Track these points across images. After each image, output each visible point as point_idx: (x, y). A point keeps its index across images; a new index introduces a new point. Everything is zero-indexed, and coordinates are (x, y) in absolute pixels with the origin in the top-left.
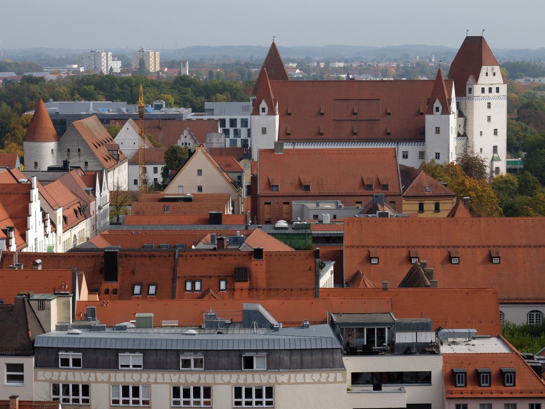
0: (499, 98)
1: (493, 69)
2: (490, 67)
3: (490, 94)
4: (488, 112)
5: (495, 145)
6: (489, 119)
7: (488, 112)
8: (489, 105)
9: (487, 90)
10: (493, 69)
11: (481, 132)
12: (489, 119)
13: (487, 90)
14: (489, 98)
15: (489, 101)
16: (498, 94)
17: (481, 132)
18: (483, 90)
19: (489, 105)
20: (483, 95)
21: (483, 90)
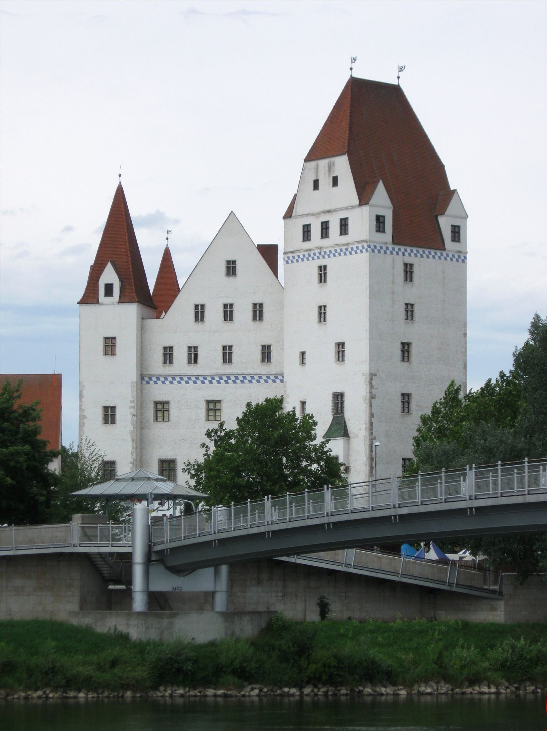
0: (347, 250)
1: (330, 167)
2: (323, 163)
3: (325, 242)
4: (319, 295)
5: (339, 390)
6: (322, 313)
7: (319, 295)
8: (322, 274)
9: (316, 231)
10: (330, 167)
11: (303, 354)
12: (322, 313)
13: (316, 231)
14: (321, 252)
15: (322, 262)
16: (344, 239)
17: (303, 354)
18: (306, 231)
19: (322, 274)
20: (307, 245)
21: (306, 231)
